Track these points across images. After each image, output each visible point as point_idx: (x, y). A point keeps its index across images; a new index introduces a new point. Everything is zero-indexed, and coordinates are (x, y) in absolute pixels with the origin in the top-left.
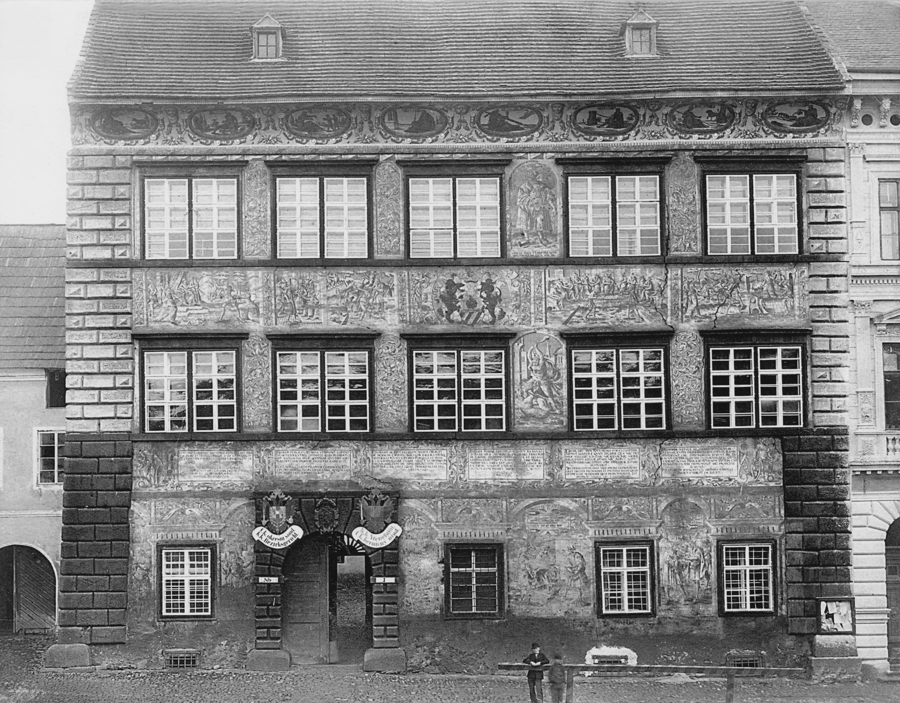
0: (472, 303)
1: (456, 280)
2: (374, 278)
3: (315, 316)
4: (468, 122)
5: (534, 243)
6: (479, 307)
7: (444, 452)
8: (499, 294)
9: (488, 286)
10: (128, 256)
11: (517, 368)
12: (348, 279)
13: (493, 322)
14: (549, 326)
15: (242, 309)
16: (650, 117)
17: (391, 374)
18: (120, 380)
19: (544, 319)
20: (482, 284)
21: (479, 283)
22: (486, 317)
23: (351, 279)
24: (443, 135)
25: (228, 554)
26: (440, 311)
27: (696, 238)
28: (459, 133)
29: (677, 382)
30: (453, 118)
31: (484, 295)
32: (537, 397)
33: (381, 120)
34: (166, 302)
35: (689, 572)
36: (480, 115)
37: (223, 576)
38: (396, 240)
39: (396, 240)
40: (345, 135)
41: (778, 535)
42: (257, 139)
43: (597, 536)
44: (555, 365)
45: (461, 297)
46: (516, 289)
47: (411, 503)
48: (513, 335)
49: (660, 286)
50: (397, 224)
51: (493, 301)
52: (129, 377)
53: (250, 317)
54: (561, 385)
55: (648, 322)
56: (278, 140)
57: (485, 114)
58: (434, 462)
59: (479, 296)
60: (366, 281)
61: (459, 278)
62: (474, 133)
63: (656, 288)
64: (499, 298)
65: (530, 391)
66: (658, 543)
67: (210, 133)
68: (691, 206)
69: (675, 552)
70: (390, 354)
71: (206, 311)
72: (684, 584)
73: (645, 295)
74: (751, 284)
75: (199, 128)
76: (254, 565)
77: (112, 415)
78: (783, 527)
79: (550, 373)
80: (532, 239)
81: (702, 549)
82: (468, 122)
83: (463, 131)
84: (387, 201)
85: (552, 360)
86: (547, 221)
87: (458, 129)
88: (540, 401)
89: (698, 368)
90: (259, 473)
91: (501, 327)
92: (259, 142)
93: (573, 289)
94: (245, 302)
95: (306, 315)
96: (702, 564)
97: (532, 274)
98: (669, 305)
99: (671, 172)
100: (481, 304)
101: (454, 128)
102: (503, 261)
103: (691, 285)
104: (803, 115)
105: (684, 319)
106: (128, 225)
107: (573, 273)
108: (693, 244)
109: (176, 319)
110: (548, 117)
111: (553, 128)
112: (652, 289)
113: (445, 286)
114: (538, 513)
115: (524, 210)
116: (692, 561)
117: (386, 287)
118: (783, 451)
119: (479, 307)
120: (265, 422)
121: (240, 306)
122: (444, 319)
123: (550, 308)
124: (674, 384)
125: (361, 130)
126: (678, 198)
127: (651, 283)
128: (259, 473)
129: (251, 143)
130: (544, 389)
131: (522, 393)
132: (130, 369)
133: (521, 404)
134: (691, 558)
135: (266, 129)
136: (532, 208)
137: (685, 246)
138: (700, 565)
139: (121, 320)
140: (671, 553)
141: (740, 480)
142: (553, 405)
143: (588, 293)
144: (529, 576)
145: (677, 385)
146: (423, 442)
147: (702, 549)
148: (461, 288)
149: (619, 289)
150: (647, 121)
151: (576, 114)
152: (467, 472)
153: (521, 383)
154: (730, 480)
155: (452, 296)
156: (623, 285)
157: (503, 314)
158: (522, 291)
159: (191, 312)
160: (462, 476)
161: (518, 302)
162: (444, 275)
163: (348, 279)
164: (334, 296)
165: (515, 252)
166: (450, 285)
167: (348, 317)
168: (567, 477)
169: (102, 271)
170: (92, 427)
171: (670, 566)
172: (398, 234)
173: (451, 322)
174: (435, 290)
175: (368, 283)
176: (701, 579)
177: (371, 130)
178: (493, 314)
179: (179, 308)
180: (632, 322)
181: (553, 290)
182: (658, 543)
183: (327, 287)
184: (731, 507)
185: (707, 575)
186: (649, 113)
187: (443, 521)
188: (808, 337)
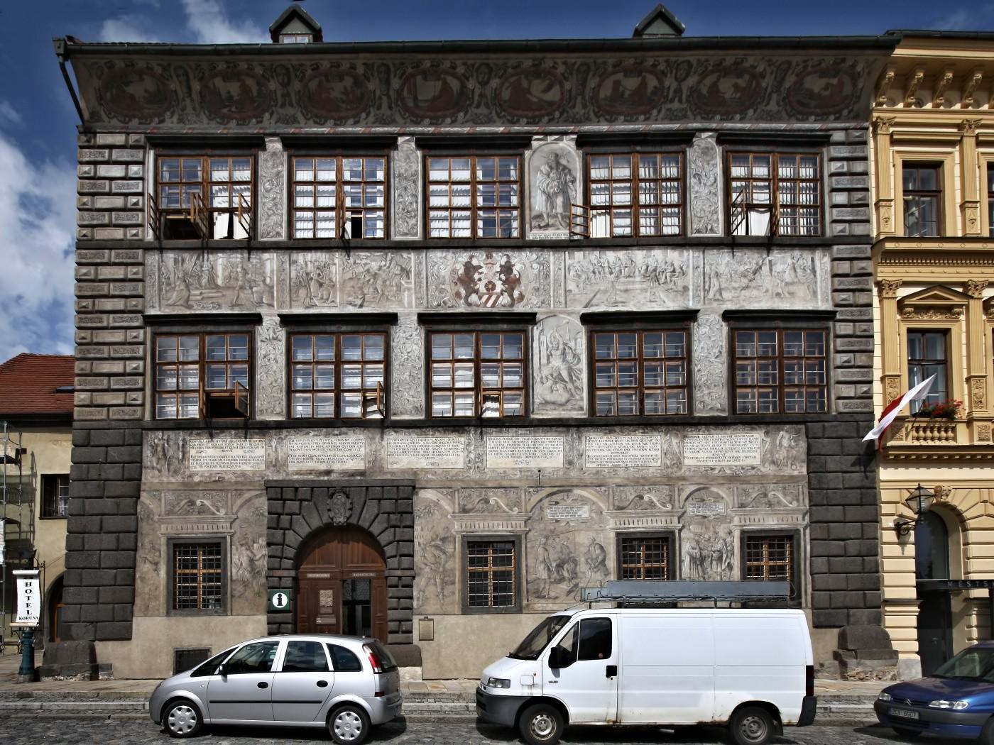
0: (490, 286)
1: (475, 262)
2: (391, 261)
3: (330, 300)
4: (489, 97)
5: (553, 225)
6: (498, 290)
7: (462, 439)
8: (518, 277)
9: (507, 269)
10: (140, 237)
11: (536, 351)
12: (364, 261)
13: (512, 305)
14: (570, 309)
15: (256, 292)
16: (675, 91)
17: (408, 359)
18: (132, 365)
19: (564, 302)
20: (501, 266)
21: (498, 265)
22: (505, 299)
23: (368, 261)
24: (462, 114)
25: (239, 546)
26: (458, 294)
27: (718, 219)
28: (479, 111)
29: (699, 367)
30: (473, 90)
31: (503, 276)
32: (556, 383)
33: (399, 93)
34: (179, 285)
35: (711, 563)
36: (502, 84)
37: (234, 571)
38: (414, 221)
39: (414, 221)
40: (364, 115)
41: (801, 524)
42: (275, 117)
43: (618, 526)
44: (575, 350)
45: (480, 280)
46: (536, 271)
47: (427, 495)
48: (530, 318)
49: (681, 268)
50: (414, 204)
51: (511, 282)
52: (141, 363)
53: (264, 300)
54: (580, 370)
55: (670, 304)
56: (294, 121)
57: (507, 84)
58: (451, 451)
59: (497, 278)
60: (383, 263)
61: (479, 258)
62: (494, 112)
63: (678, 270)
64: (518, 281)
65: (550, 377)
66: (679, 534)
67: (225, 110)
68: (712, 188)
69: (698, 542)
70: (407, 339)
71: (220, 294)
72: (706, 576)
73: (666, 278)
74: (774, 267)
75: (213, 105)
76: (266, 558)
77: (121, 401)
78: (807, 518)
79: (569, 358)
80: (551, 221)
81: (725, 540)
82: (489, 97)
83: (483, 110)
84: (404, 183)
85: (572, 344)
86: (568, 204)
87: (478, 106)
88: (560, 386)
89: (721, 352)
90: (271, 462)
91: (519, 308)
92: (276, 122)
93: (594, 272)
94: (259, 285)
95: (322, 298)
96: (725, 556)
97: (552, 258)
98: (691, 288)
99: (692, 153)
100: (499, 287)
101: (474, 105)
102: (523, 245)
103: (713, 267)
104: (827, 93)
105: (706, 302)
106: (141, 203)
107: (594, 256)
108: (715, 225)
109: (190, 303)
110: (570, 91)
111: (574, 107)
112: (674, 271)
113: (463, 268)
114: (557, 503)
115: (544, 192)
116: (714, 552)
117: (403, 269)
118: (807, 437)
119: (498, 290)
120: (278, 410)
121: (254, 289)
122: (462, 301)
123: (570, 291)
124: (696, 369)
125: (379, 108)
126: (699, 179)
127: (672, 265)
128: (271, 462)
129: (269, 124)
130: (565, 374)
131: (542, 378)
132: (141, 353)
133: (541, 391)
134: (714, 549)
135: (283, 106)
136: (552, 191)
137: (706, 228)
138: (722, 556)
139: (134, 302)
140: (694, 544)
141: (762, 469)
142: (573, 390)
143: (608, 276)
144: (549, 569)
145: (699, 371)
146: (440, 429)
147: (725, 540)
148: (480, 271)
149: (640, 271)
150: (670, 96)
151: (600, 85)
152: (485, 463)
153: (540, 368)
154: (753, 468)
155: (471, 280)
156: (644, 267)
157: (522, 297)
158: (542, 274)
159: (205, 295)
160: (480, 465)
161: (537, 285)
162: (463, 257)
163: (364, 261)
164: (351, 279)
165: (533, 235)
166: (470, 268)
167: (364, 300)
168: (587, 465)
169: (113, 252)
170: (102, 414)
171: (693, 558)
172: (416, 216)
173: (470, 305)
174: (454, 271)
175: (385, 265)
176: (724, 570)
177: (390, 108)
178: (511, 296)
179: (193, 292)
180: (653, 304)
181: (572, 273)
182: (679, 534)
183: (343, 269)
184: (753, 496)
185: (730, 567)
186: (674, 85)
187: (460, 512)
188: (831, 324)
